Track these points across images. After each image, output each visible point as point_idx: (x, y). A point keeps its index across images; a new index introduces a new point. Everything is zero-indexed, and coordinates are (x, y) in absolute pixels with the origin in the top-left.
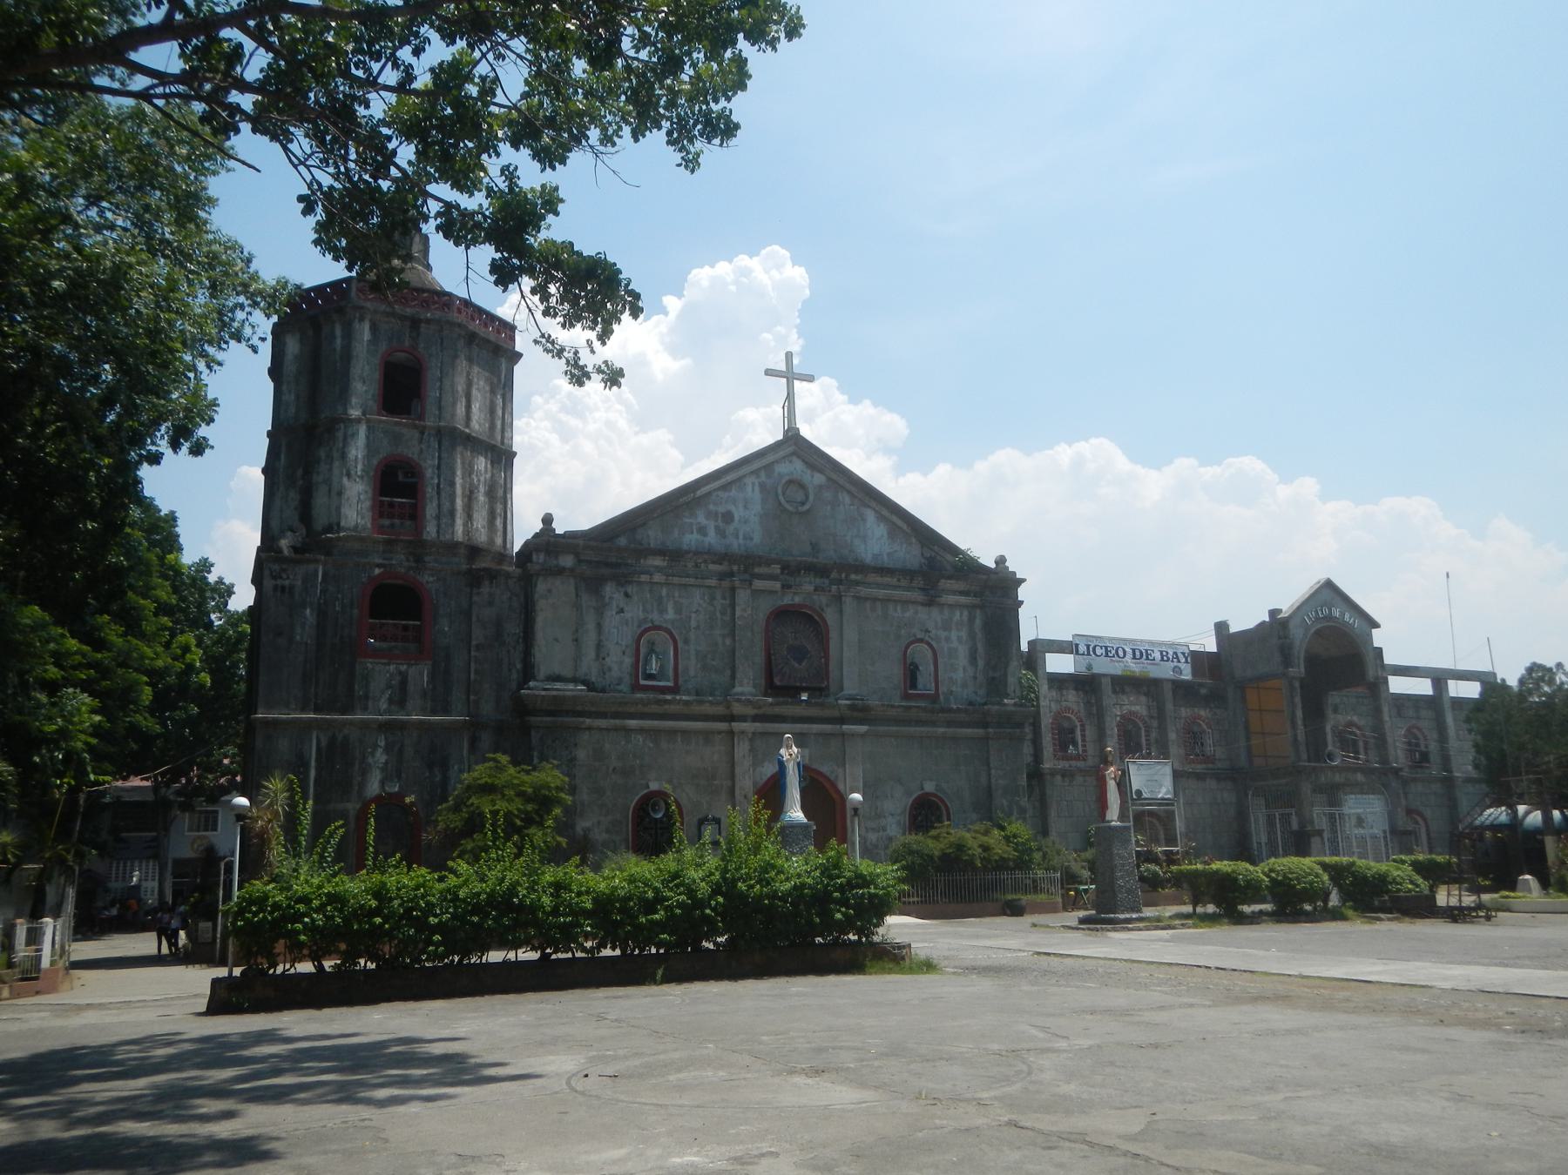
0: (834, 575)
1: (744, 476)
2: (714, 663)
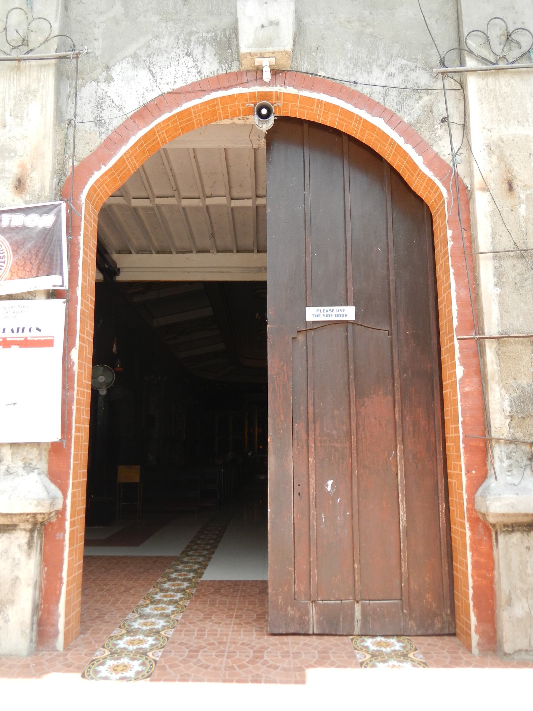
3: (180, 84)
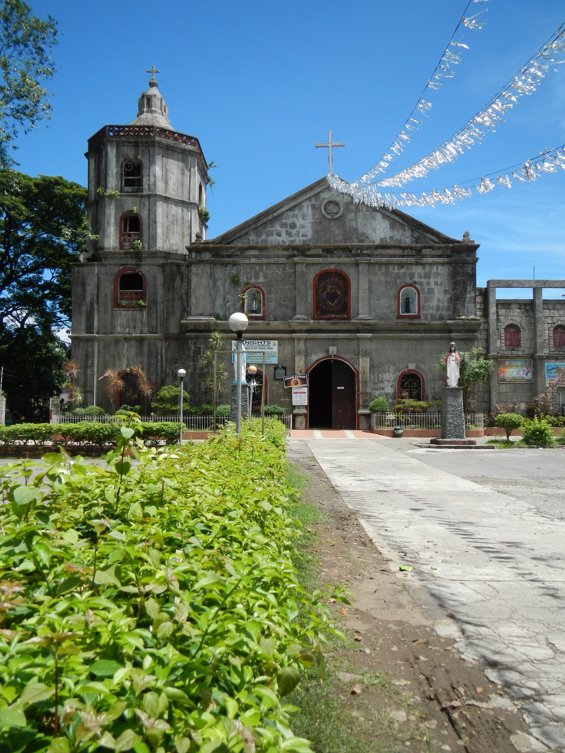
0: (354, 252)
1: (302, 202)
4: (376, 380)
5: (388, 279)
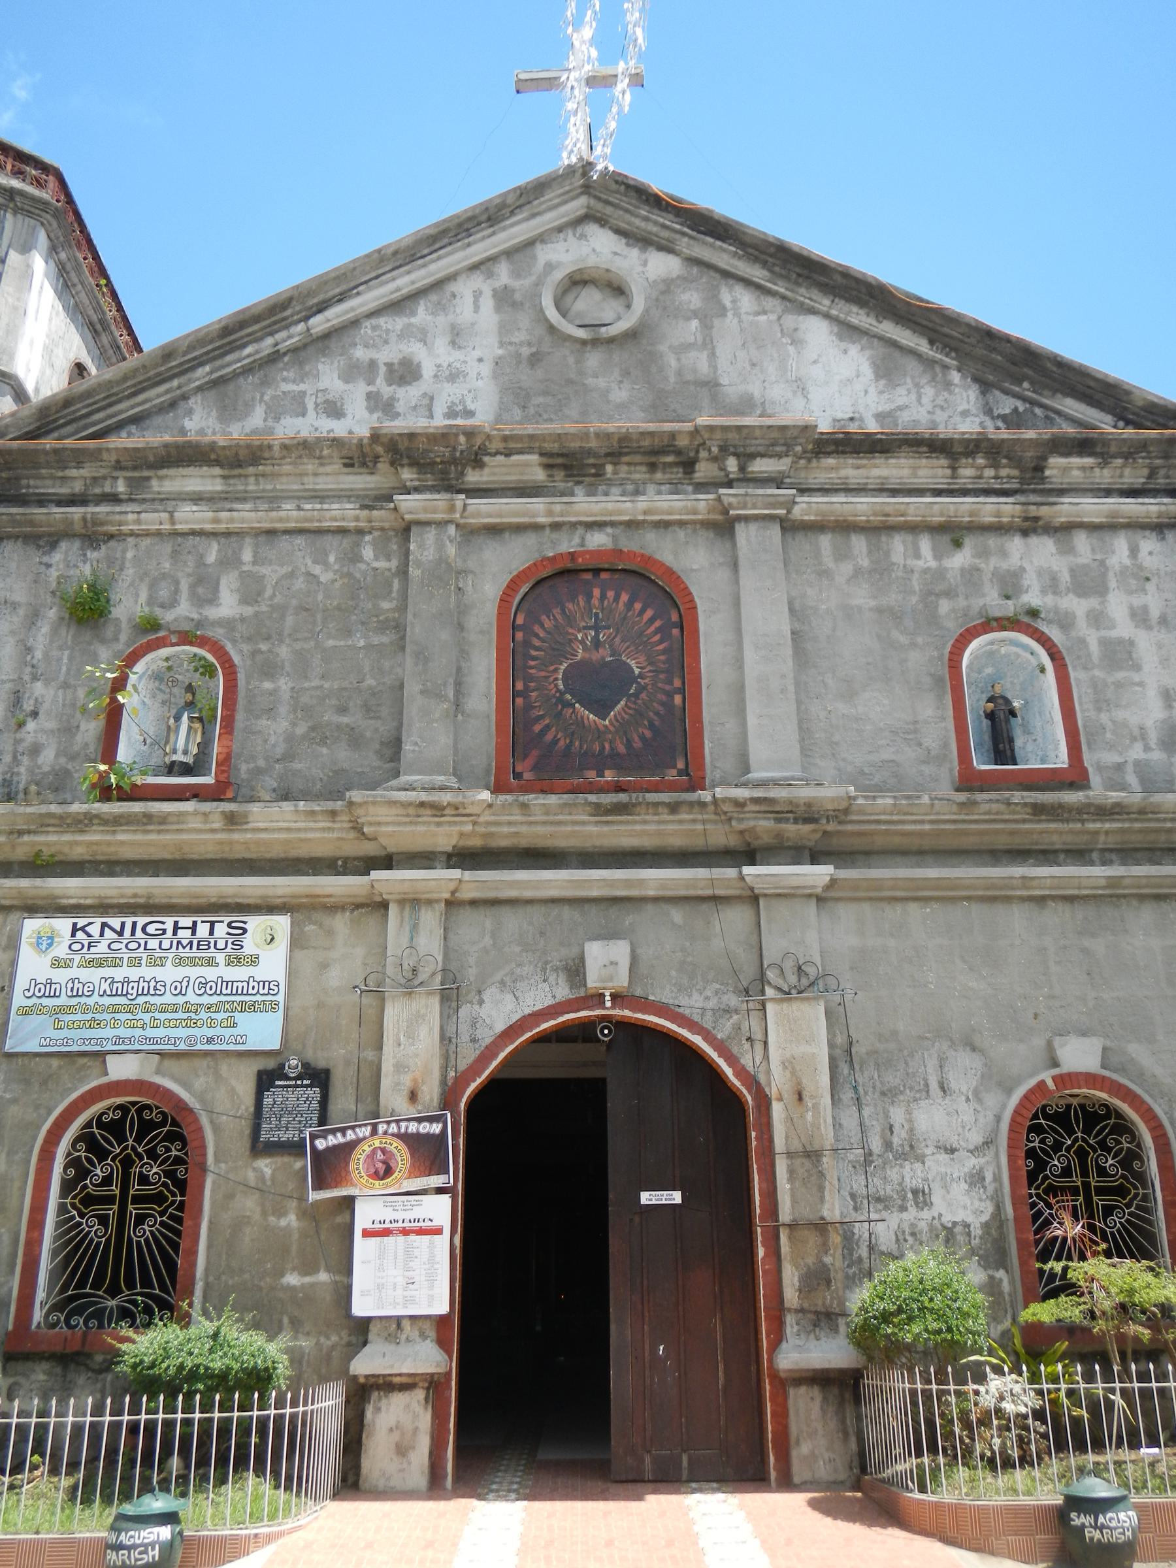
0: (704, 470)
1: (452, 277)
2: (345, 720)
3: (538, 1007)
4: (876, 1145)
5: (892, 598)
